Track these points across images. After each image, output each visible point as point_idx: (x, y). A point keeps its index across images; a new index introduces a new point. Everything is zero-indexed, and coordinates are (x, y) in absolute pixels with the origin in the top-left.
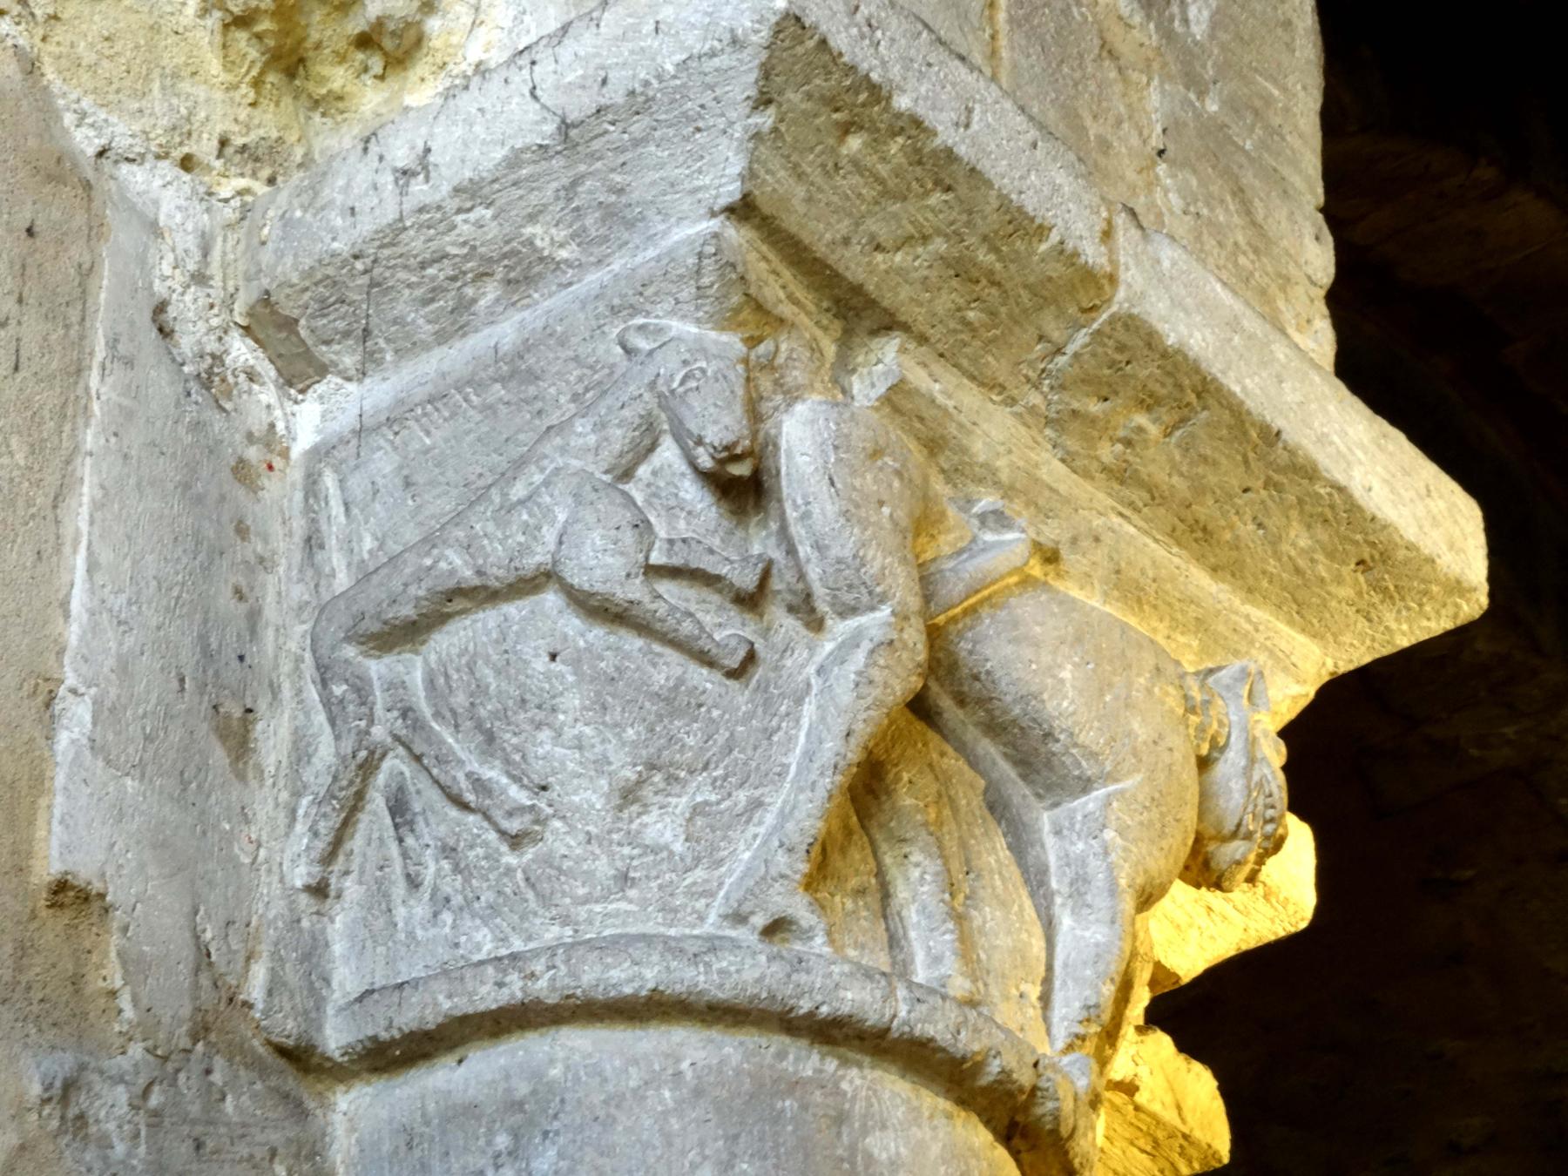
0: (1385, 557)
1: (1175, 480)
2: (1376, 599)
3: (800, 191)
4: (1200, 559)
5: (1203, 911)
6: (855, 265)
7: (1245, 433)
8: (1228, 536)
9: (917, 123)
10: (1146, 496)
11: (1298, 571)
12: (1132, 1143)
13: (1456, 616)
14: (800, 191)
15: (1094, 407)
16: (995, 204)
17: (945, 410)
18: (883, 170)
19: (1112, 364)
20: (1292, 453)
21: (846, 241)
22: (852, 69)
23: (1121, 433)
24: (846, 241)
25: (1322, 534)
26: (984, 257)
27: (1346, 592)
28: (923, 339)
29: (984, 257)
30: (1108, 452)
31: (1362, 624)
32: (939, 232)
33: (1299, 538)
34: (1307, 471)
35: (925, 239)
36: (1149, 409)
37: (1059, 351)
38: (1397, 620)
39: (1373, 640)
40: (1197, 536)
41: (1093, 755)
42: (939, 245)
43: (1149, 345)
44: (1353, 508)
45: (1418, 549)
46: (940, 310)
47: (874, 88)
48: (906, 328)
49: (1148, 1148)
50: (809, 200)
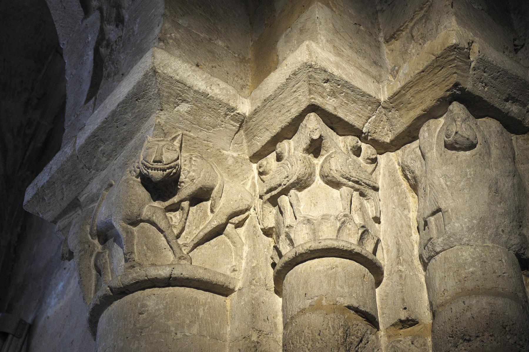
0: (136, 94)
1: (112, 144)
2: (146, 97)
3: (52, 211)
4: (129, 142)
5: (295, 93)
6: (65, 204)
7: (104, 127)
8: (125, 133)
9: (43, 186)
10: (114, 152)
11: (135, 117)
12: (436, 74)
13: (153, 76)
14: (52, 211)
15: (95, 160)
16: (56, 174)
17: (88, 195)
18: (50, 195)
19: (87, 155)
20: (109, 116)
21: (61, 205)
22: (33, 197)
23: (102, 155)
24: (61, 205)
25: (129, 110)
26: (66, 178)
27: (143, 104)
28: (79, 194)
29: (66, 178)
30: (104, 159)
31: (151, 102)
32: (61, 186)
33: (129, 116)
34: (114, 113)
35: (62, 189)
36: (98, 147)
37: (85, 165)
38: (151, 92)
39: (155, 99)
40: (125, 141)
41: (109, 216)
42: (64, 186)
43: (84, 147)
44: (123, 102)
45: (135, 86)
46: (74, 189)
47: (36, 194)
48: (77, 197)
49: (440, 68)
50: (53, 210)
